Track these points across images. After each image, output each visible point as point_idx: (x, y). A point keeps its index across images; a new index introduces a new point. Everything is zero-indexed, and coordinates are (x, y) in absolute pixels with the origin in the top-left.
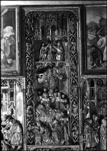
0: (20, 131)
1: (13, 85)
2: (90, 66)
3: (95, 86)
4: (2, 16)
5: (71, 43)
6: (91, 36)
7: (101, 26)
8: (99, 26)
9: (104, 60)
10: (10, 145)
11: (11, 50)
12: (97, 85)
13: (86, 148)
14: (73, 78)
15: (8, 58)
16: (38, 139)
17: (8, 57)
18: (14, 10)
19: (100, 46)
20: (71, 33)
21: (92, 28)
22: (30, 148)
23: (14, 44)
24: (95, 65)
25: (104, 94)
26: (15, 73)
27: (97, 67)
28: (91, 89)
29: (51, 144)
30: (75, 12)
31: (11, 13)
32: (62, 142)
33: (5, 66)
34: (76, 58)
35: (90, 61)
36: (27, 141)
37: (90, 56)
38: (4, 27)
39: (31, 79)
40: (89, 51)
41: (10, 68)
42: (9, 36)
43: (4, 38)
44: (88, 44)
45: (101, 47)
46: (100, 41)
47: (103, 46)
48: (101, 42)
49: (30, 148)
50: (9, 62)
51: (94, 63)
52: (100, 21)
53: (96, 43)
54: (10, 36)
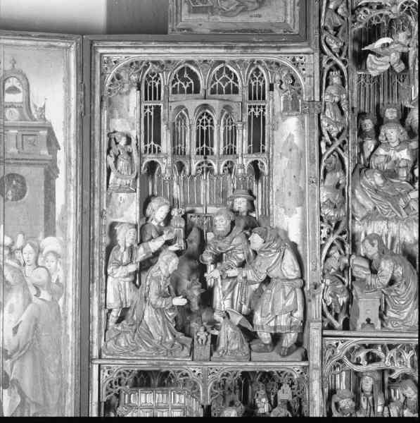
0: (295, 271)
1: (259, 87)
10: (250, 327)
16: (367, 307)
22: (337, 344)
26: (281, 32)
36: (324, 315)
39: (341, 64)
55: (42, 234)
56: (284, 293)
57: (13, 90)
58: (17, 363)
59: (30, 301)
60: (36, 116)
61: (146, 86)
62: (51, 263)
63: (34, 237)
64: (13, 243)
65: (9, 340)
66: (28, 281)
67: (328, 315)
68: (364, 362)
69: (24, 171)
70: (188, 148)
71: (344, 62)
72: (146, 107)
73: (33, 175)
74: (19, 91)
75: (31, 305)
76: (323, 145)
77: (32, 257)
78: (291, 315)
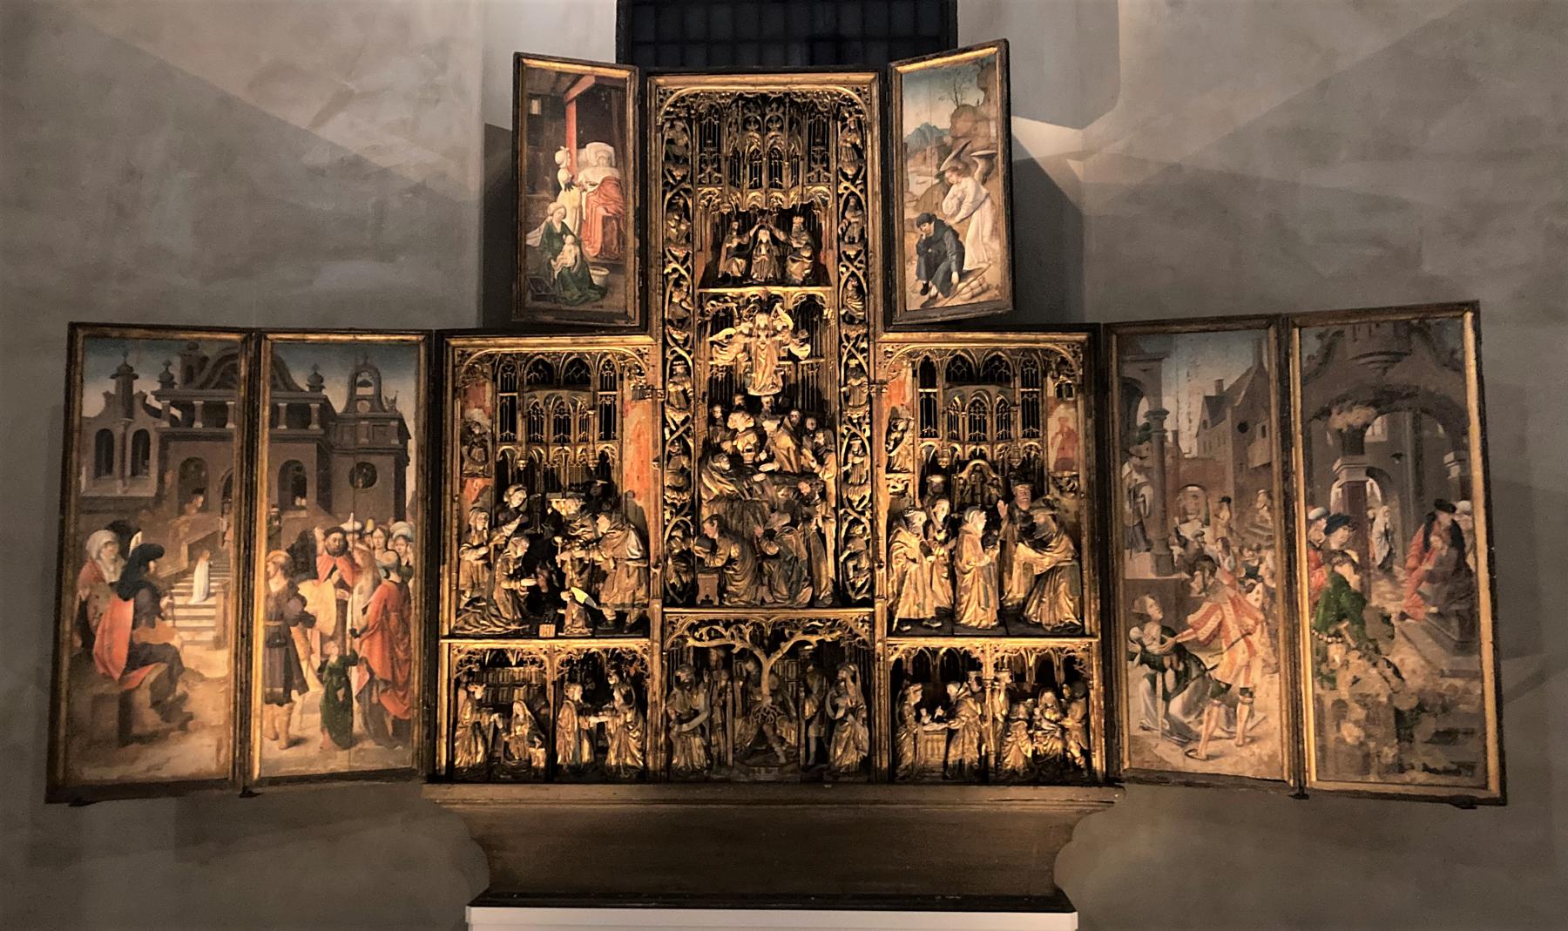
0: (639, 550)
2: (914, 296)
3: (941, 380)
4: (571, 101)
5: (844, 217)
6: (918, 180)
7: (956, 138)
8: (948, 140)
9: (966, 268)
11: (604, 234)
12: (948, 380)
13: (899, 619)
14: (850, 351)
15: (593, 264)
16: (707, 585)
17: (595, 260)
18: (621, 85)
19: (953, 216)
20: (845, 176)
21: (925, 150)
23: (619, 213)
24: (934, 291)
27: (940, 300)
28: (921, 394)
29: (758, 603)
30: (860, 95)
31: (610, 94)
32: (806, 594)
33: (580, 294)
34: (861, 271)
35: (916, 277)
37: (916, 257)
38: (581, 145)
40: (912, 241)
41: (600, 303)
42: (599, 182)
43: (580, 185)
44: (910, 214)
45: (958, 218)
46: (955, 196)
47: (962, 214)
48: (955, 201)
49: (674, 619)
50: (596, 280)
51: (930, 284)
52: (955, 116)
53: (938, 206)
54: (603, 181)
55: (392, 520)
56: (628, 572)
57: (365, 384)
58: (366, 641)
59: (379, 582)
60: (387, 408)
61: (502, 377)
62: (401, 546)
63: (385, 523)
64: (364, 528)
65: (358, 621)
66: (378, 564)
67: (671, 592)
68: (705, 637)
69: (374, 460)
70: (545, 436)
71: (689, 353)
72: (502, 398)
73: (384, 465)
74: (370, 385)
75: (380, 587)
76: (667, 431)
77: (382, 541)
78: (634, 593)
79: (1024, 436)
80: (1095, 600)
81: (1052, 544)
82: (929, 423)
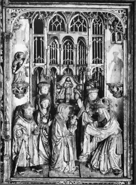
3: (46, 31)
25: (67, 53)
79: (93, 63)
80: (130, 158)
81: (107, 125)
82: (39, 54)
